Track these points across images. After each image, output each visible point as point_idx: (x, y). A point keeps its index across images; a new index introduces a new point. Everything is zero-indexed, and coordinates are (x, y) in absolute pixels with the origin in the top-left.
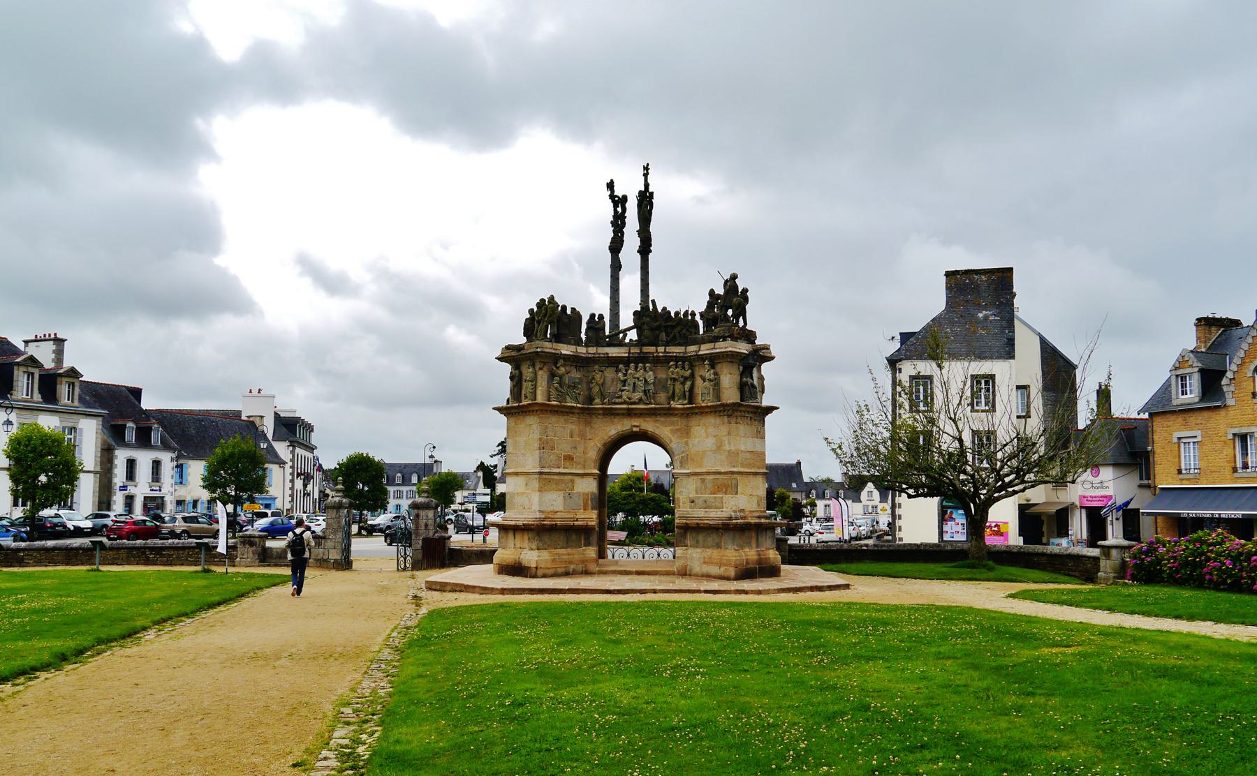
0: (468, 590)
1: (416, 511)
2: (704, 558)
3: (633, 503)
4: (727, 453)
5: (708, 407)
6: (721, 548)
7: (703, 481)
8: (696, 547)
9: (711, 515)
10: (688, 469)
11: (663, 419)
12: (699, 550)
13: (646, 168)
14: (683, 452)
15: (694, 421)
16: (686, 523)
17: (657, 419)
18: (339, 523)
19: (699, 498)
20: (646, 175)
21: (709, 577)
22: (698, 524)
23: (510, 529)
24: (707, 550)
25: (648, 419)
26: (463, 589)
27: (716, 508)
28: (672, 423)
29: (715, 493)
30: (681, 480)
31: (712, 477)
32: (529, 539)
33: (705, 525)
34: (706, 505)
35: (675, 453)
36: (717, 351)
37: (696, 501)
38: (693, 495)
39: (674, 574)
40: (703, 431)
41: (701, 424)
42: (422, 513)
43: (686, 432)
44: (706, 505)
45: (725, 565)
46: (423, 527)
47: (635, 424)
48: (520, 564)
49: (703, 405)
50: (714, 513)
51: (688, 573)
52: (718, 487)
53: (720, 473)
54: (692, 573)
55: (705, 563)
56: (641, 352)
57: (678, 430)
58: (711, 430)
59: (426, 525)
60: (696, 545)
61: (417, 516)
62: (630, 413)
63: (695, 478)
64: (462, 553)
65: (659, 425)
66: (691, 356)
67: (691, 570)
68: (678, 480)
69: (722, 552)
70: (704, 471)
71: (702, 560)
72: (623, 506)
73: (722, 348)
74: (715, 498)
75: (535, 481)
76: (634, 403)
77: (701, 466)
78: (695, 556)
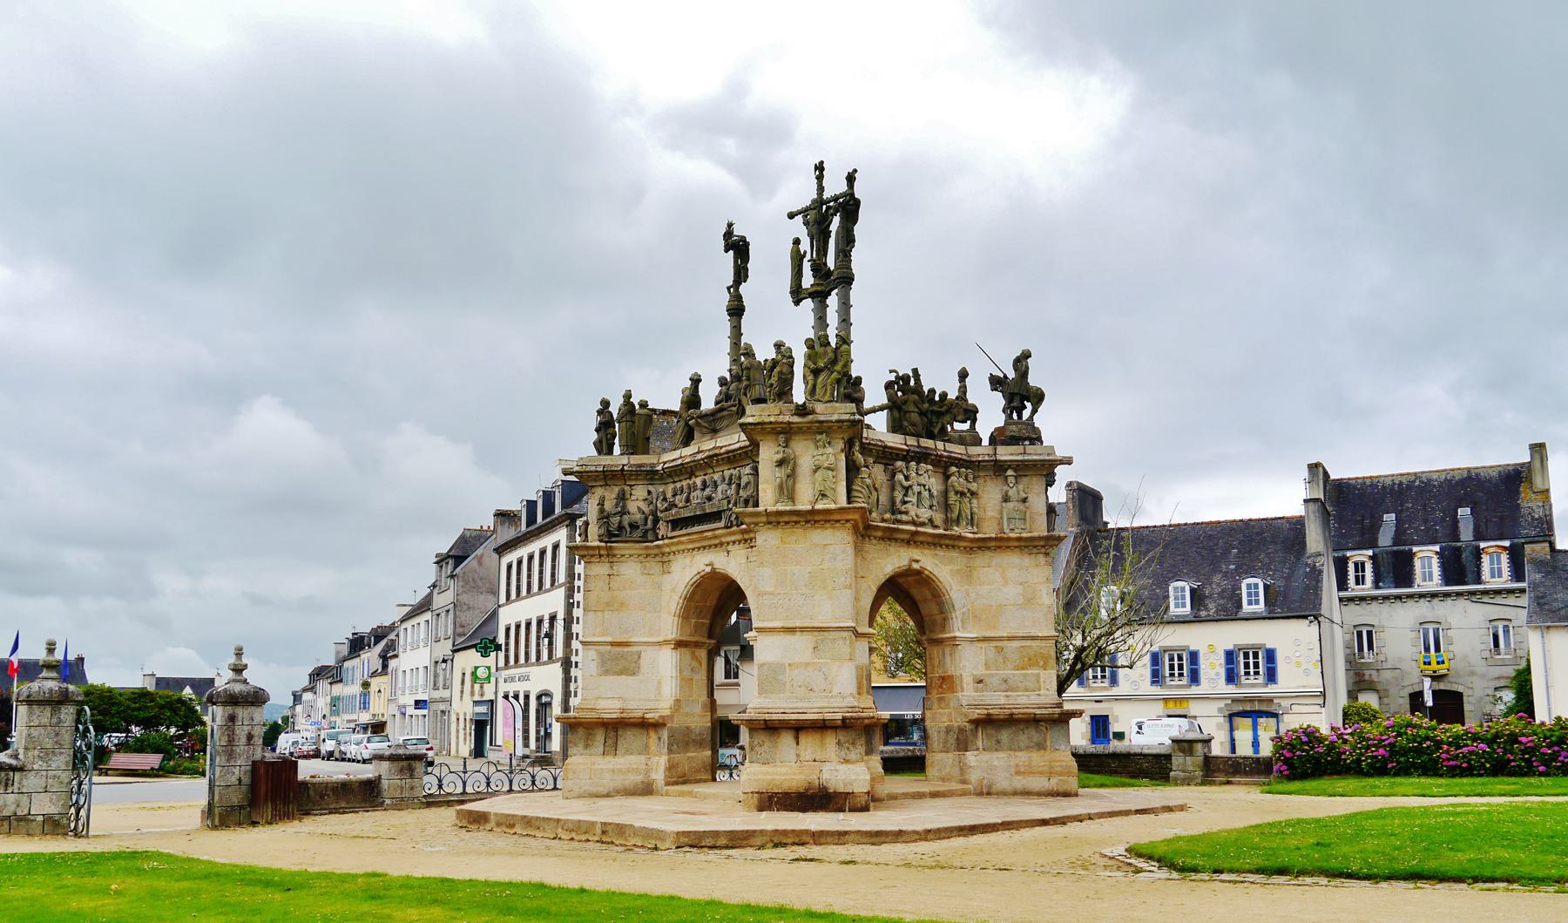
0: (822, 840)
1: (229, 709)
3: (152, 708)
4: (1046, 609)
5: (1019, 539)
6: (1045, 749)
7: (1000, 650)
8: (996, 750)
9: (1021, 702)
10: (970, 632)
11: (941, 553)
12: (1001, 755)
15: (981, 559)
16: (988, 715)
17: (936, 552)
18: (57, 735)
19: (992, 676)
20: (820, 178)
21: (1026, 793)
22: (1012, 714)
24: (1019, 754)
25: (926, 551)
26: (808, 839)
27: (1027, 690)
29: (1023, 669)
30: (964, 647)
31: (1016, 644)
32: (839, 743)
34: (1007, 686)
35: (957, 606)
36: (1030, 458)
37: (987, 680)
38: (981, 671)
39: (970, 794)
40: (997, 575)
41: (993, 564)
42: (242, 713)
43: (968, 575)
45: (1060, 774)
46: (243, 740)
47: (917, 557)
48: (825, 788)
49: (1012, 535)
50: (1024, 698)
53: (1034, 638)
54: (993, 790)
55: (1018, 773)
56: (919, 446)
57: (959, 571)
59: (250, 737)
60: (998, 746)
61: (232, 718)
62: (913, 540)
63: (984, 645)
64: (308, 788)
65: (937, 562)
66: (980, 462)
67: (990, 787)
68: (959, 647)
70: (1005, 635)
71: (1013, 770)
72: (136, 713)
73: (1040, 454)
74: (1025, 675)
75: (841, 642)
76: (922, 524)
78: (996, 763)
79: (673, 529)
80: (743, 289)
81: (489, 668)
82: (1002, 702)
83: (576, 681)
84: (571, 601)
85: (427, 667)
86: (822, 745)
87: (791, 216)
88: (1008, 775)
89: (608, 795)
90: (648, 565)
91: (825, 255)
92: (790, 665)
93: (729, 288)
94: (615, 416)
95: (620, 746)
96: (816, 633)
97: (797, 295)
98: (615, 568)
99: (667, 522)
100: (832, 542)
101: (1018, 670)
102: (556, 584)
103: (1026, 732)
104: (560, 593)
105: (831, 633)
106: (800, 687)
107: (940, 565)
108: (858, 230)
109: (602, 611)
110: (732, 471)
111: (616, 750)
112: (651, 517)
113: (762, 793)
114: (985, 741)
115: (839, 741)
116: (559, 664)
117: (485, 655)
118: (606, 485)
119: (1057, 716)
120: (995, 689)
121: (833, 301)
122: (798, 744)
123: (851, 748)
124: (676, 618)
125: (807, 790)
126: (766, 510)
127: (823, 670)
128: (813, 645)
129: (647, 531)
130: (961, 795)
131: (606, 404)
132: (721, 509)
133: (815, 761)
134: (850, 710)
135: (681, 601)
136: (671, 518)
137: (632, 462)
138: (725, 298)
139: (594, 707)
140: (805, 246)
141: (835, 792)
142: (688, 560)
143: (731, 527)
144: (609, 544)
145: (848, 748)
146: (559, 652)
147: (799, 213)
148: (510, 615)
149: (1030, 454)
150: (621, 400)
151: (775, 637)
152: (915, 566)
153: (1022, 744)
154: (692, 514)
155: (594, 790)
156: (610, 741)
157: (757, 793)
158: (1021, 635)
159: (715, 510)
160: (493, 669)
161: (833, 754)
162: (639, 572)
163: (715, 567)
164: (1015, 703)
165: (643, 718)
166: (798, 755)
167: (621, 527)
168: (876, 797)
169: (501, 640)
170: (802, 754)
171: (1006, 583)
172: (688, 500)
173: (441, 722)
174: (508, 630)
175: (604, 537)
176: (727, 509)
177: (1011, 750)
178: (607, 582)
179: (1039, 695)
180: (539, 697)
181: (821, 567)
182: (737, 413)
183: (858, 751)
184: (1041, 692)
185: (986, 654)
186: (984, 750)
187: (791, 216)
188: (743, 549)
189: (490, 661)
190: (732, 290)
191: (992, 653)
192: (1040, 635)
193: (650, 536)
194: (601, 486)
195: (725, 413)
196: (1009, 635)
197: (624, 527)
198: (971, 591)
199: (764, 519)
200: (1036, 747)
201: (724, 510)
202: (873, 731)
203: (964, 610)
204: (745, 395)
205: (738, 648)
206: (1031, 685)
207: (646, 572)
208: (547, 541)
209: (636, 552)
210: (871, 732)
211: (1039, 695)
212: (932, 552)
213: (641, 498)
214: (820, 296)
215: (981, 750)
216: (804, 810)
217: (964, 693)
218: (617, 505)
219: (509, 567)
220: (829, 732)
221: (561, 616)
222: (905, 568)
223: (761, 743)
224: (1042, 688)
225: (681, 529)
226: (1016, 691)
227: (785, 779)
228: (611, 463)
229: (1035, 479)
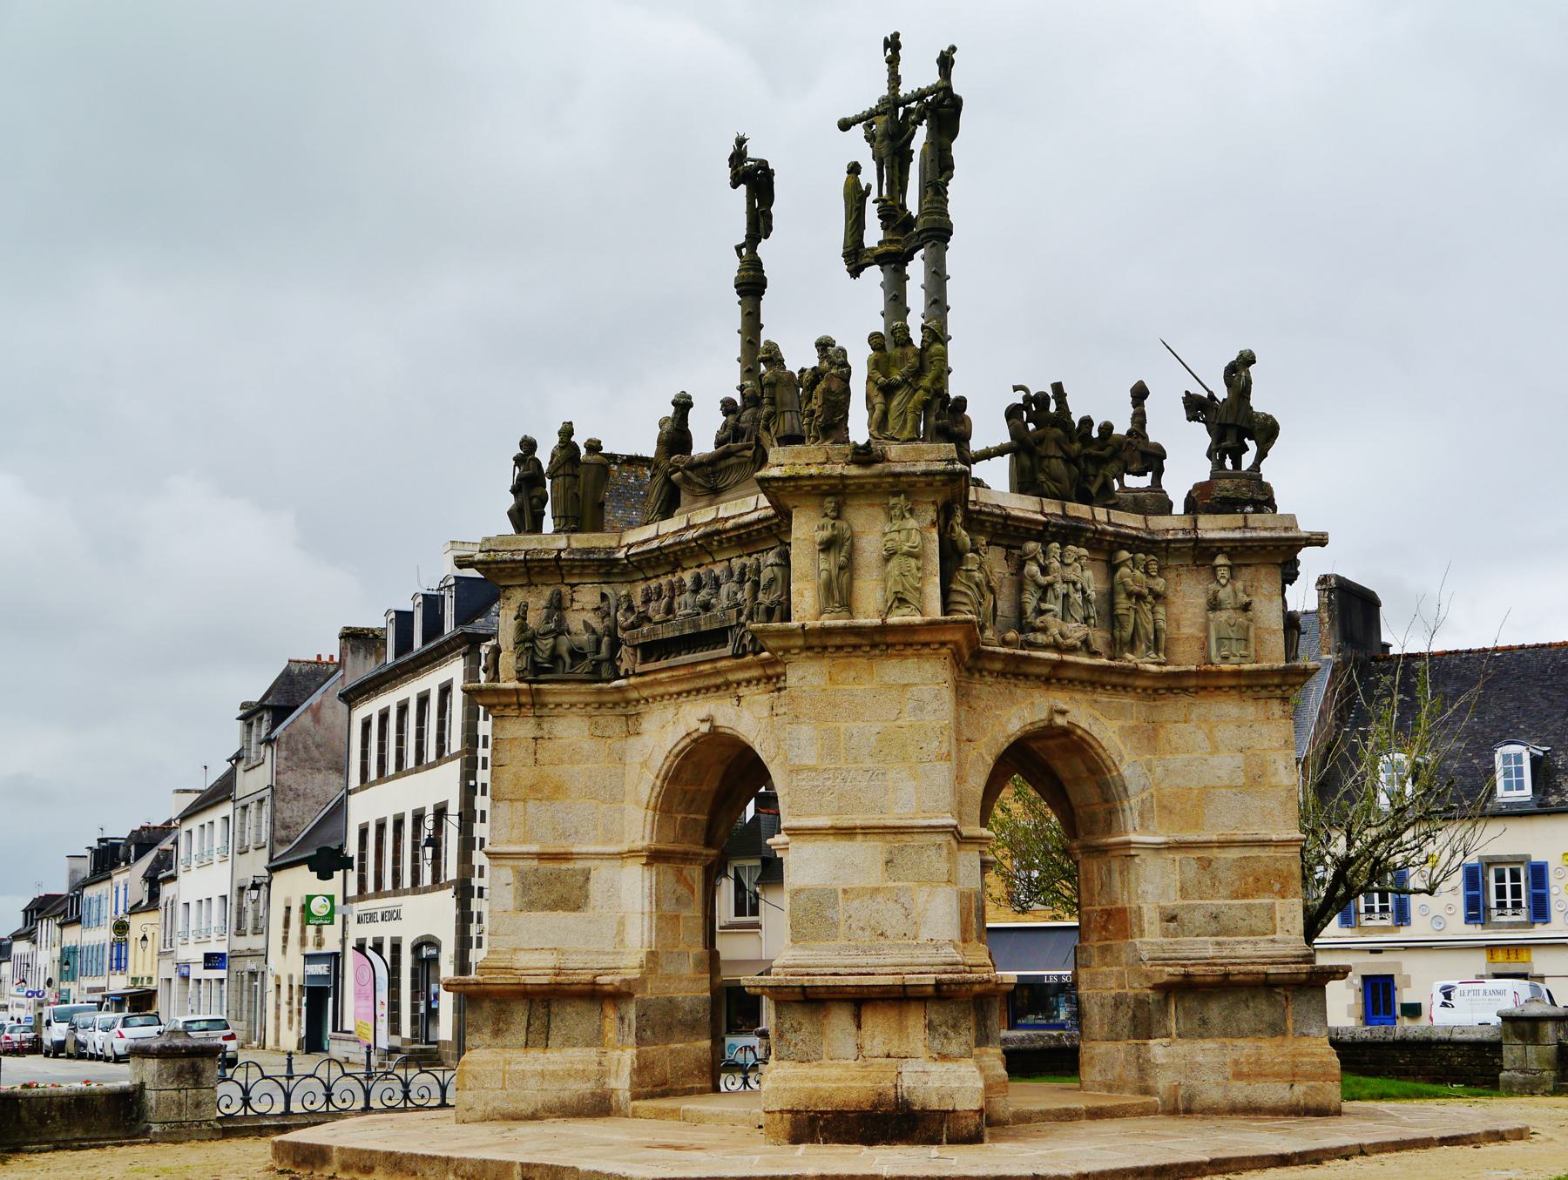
2: (1236, 1062)
4: (1284, 794)
5: (1238, 674)
6: (1284, 1033)
7: (1206, 864)
8: (1201, 1036)
9: (1243, 953)
10: (1155, 834)
11: (1104, 699)
12: (1209, 1044)
13: (893, 44)
14: (1143, 790)
15: (1171, 709)
16: (1187, 975)
17: (1095, 696)
19: (1194, 908)
20: (893, 61)
21: (1252, 1110)
22: (1227, 975)
23: (846, 1000)
24: (1240, 1042)
25: (1078, 696)
27: (1252, 933)
28: (1121, 712)
29: (1245, 896)
30: (1144, 860)
31: (1234, 854)
32: (930, 1026)
33: (1249, 978)
34: (1218, 925)
35: (1131, 791)
36: (1254, 534)
37: (1182, 914)
38: (1173, 901)
39: (1156, 1112)
40: (1200, 735)
41: (1193, 716)
43: (1149, 737)
44: (1218, 925)
45: (1309, 1077)
49: (1226, 667)
50: (1249, 946)
51: (1181, 1107)
52: (1257, 880)
53: (1264, 844)
54: (1196, 1105)
55: (1238, 1075)
56: (1065, 516)
57: (1134, 729)
58: (1226, 733)
60: (1202, 1030)
62: (1056, 677)
63: (1178, 856)
65: (1097, 714)
66: (1169, 541)
67: (1190, 1099)
68: (1137, 860)
69: (1289, 1045)
70: (1215, 838)
71: (1229, 1071)
73: (1272, 529)
74: (1248, 908)
75: (932, 852)
76: (1072, 649)
77: (1197, 825)
78: (1200, 1059)
79: (645, 660)
80: (764, 249)
81: (331, 898)
82: (1210, 953)
83: (480, 921)
84: (472, 783)
85: (225, 897)
86: (902, 1028)
87: (845, 125)
88: (1220, 1079)
89: (534, 1117)
90: (602, 721)
91: (903, 190)
92: (845, 891)
93: (739, 249)
94: (545, 467)
95: (553, 1032)
96: (889, 838)
97: (856, 259)
98: (545, 726)
99: (635, 647)
100: (917, 680)
101: (1237, 898)
102: (447, 754)
103: (1251, 1004)
104: (453, 769)
105: (916, 836)
106: (863, 929)
107: (1102, 719)
108: (958, 148)
109: (524, 800)
110: (745, 560)
111: (547, 1039)
112: (606, 639)
113: (798, 1112)
114: (1181, 1021)
115: (930, 1022)
116: (451, 891)
117: (325, 875)
118: (530, 584)
119: (1304, 976)
120: (1198, 931)
121: (916, 269)
122: (859, 1027)
123: (951, 1034)
124: (650, 813)
125: (875, 1106)
126: (803, 626)
127: (902, 900)
128: (885, 857)
129: (599, 663)
130: (1141, 1114)
131: (529, 445)
132: (727, 625)
133: (888, 1056)
134: (949, 968)
135: (659, 783)
137: (574, 545)
138: (732, 266)
139: (509, 965)
140: (869, 176)
141: (923, 1110)
142: (671, 711)
143: (743, 655)
144: (534, 686)
145: (946, 1035)
146: (451, 871)
147: (858, 120)
148: (366, 808)
149: (1255, 529)
150: (556, 440)
151: (819, 844)
152: (1060, 721)
153: (1244, 1026)
154: (677, 634)
155: (510, 1107)
156: (537, 1024)
157: (789, 1111)
158: (1241, 838)
159: (716, 626)
160: (339, 901)
161: (920, 1045)
162: (587, 733)
163: (718, 723)
164: (1233, 954)
165: (594, 983)
166: (860, 1047)
167: (555, 657)
168: (995, 1117)
169: (352, 850)
170: (867, 1044)
171: (1215, 750)
172: (670, 610)
173: (249, 991)
174: (363, 832)
175: (526, 673)
177: (1225, 1035)
178: (531, 750)
179: (1273, 941)
180: (416, 949)
181: (899, 723)
182: (754, 460)
183: (963, 1039)
184: (1278, 936)
185: (1182, 872)
186: (1179, 1036)
187: (845, 125)
189: (334, 885)
190: (744, 251)
191: (1192, 871)
192: (1274, 837)
193: (605, 671)
195: (733, 460)
196: (1222, 838)
197: (560, 657)
198: (1155, 763)
199: (800, 642)
200: (1269, 1031)
201: (731, 627)
202: (988, 1003)
203: (1145, 795)
204: (767, 429)
205: (758, 863)
206: (1258, 924)
207: (598, 732)
208: (430, 682)
209: (581, 698)
210: (985, 1009)
211: (1273, 941)
212: (1088, 697)
213: (589, 607)
214: (894, 261)
215: (1174, 1035)
216: (870, 1141)
217: (1145, 939)
218: (548, 619)
219: (366, 724)
220: (913, 1006)
221: (454, 808)
222: (1042, 724)
223: (795, 1025)
224: (1278, 929)
225: (658, 660)
226: (1235, 935)
227: (838, 1089)
228: (540, 547)
229: (1263, 571)
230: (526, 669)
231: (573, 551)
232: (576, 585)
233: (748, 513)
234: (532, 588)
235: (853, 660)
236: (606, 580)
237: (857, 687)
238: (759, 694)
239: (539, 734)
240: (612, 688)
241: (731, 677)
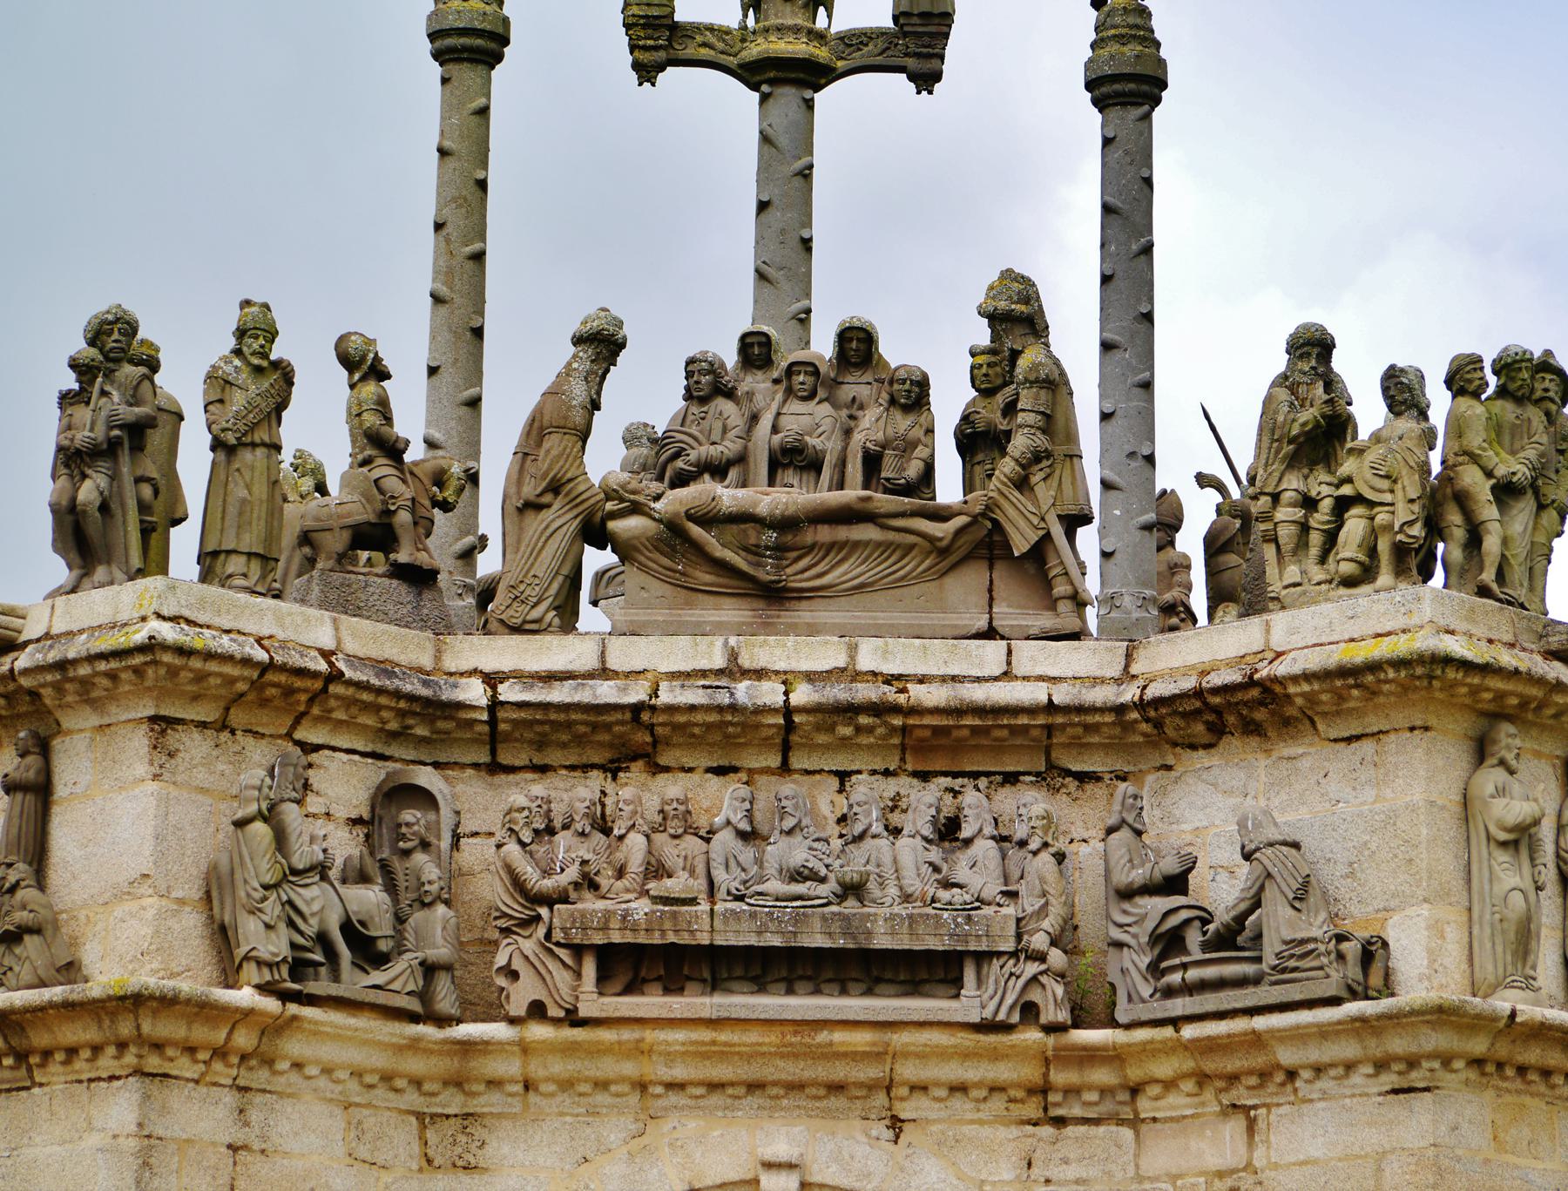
90: (370, 1121)
98: (254, 1116)
118: (223, 726)
126: (1513, 1014)
136: (598, 939)
137: (351, 646)
144: (293, 1008)
154: (776, 941)
162: (340, 1150)
176: (1014, 954)
188: (1007, 1122)
194: (203, 725)
201: (999, 954)
207: (363, 1152)
213: (342, 813)
228: (281, 635)
230: (284, 960)
231: (355, 660)
232: (317, 748)
233: (978, 680)
234: (224, 736)
235: (1527, 1100)
236: (380, 748)
237: (1533, 1164)
238: (981, 1122)
239: (239, 1136)
240: (445, 1041)
241: (908, 1071)
